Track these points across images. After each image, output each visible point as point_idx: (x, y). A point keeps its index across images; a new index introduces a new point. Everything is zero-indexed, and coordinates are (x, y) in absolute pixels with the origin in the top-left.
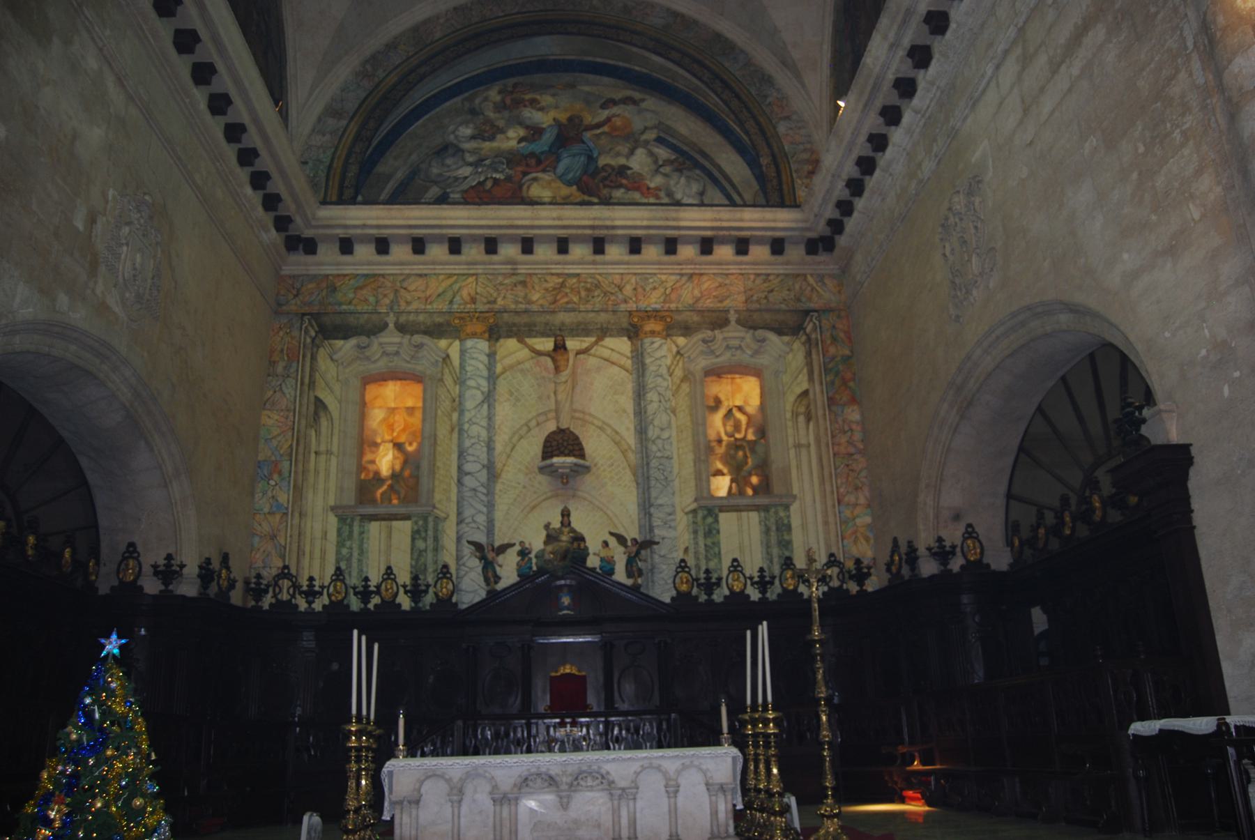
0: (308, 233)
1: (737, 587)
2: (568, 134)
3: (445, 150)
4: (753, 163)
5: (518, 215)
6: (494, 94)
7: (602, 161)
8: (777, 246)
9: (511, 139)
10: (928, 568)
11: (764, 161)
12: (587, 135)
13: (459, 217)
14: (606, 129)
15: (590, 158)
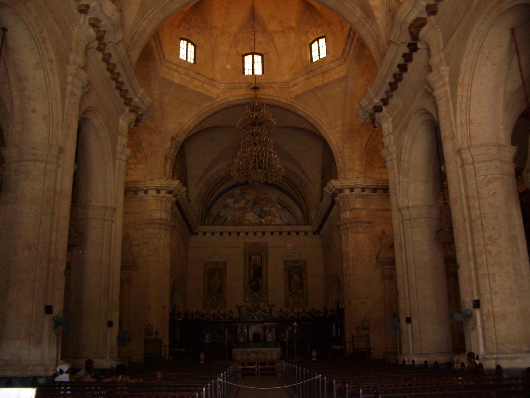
0: (196, 231)
1: (293, 315)
2: (256, 202)
3: (226, 206)
4: (301, 209)
5: (245, 228)
6: (237, 191)
7: (265, 209)
8: (306, 233)
9: (242, 204)
10: (330, 314)
11: (305, 208)
12: (261, 202)
13: (231, 228)
14: (265, 200)
15: (262, 208)
